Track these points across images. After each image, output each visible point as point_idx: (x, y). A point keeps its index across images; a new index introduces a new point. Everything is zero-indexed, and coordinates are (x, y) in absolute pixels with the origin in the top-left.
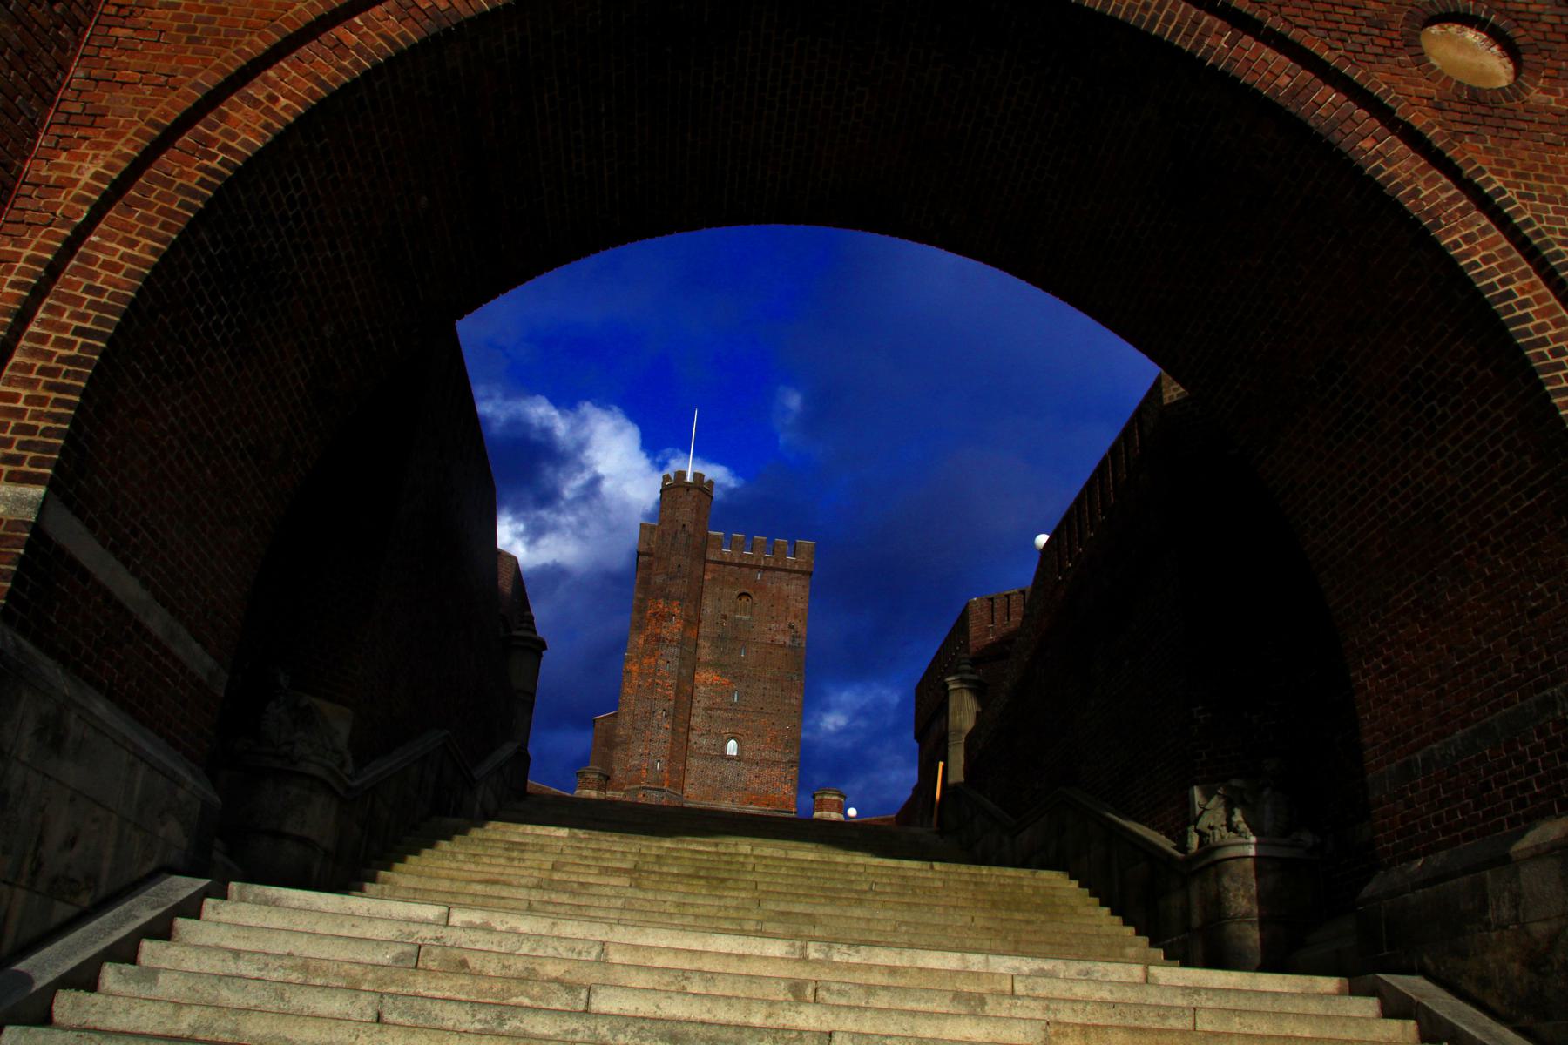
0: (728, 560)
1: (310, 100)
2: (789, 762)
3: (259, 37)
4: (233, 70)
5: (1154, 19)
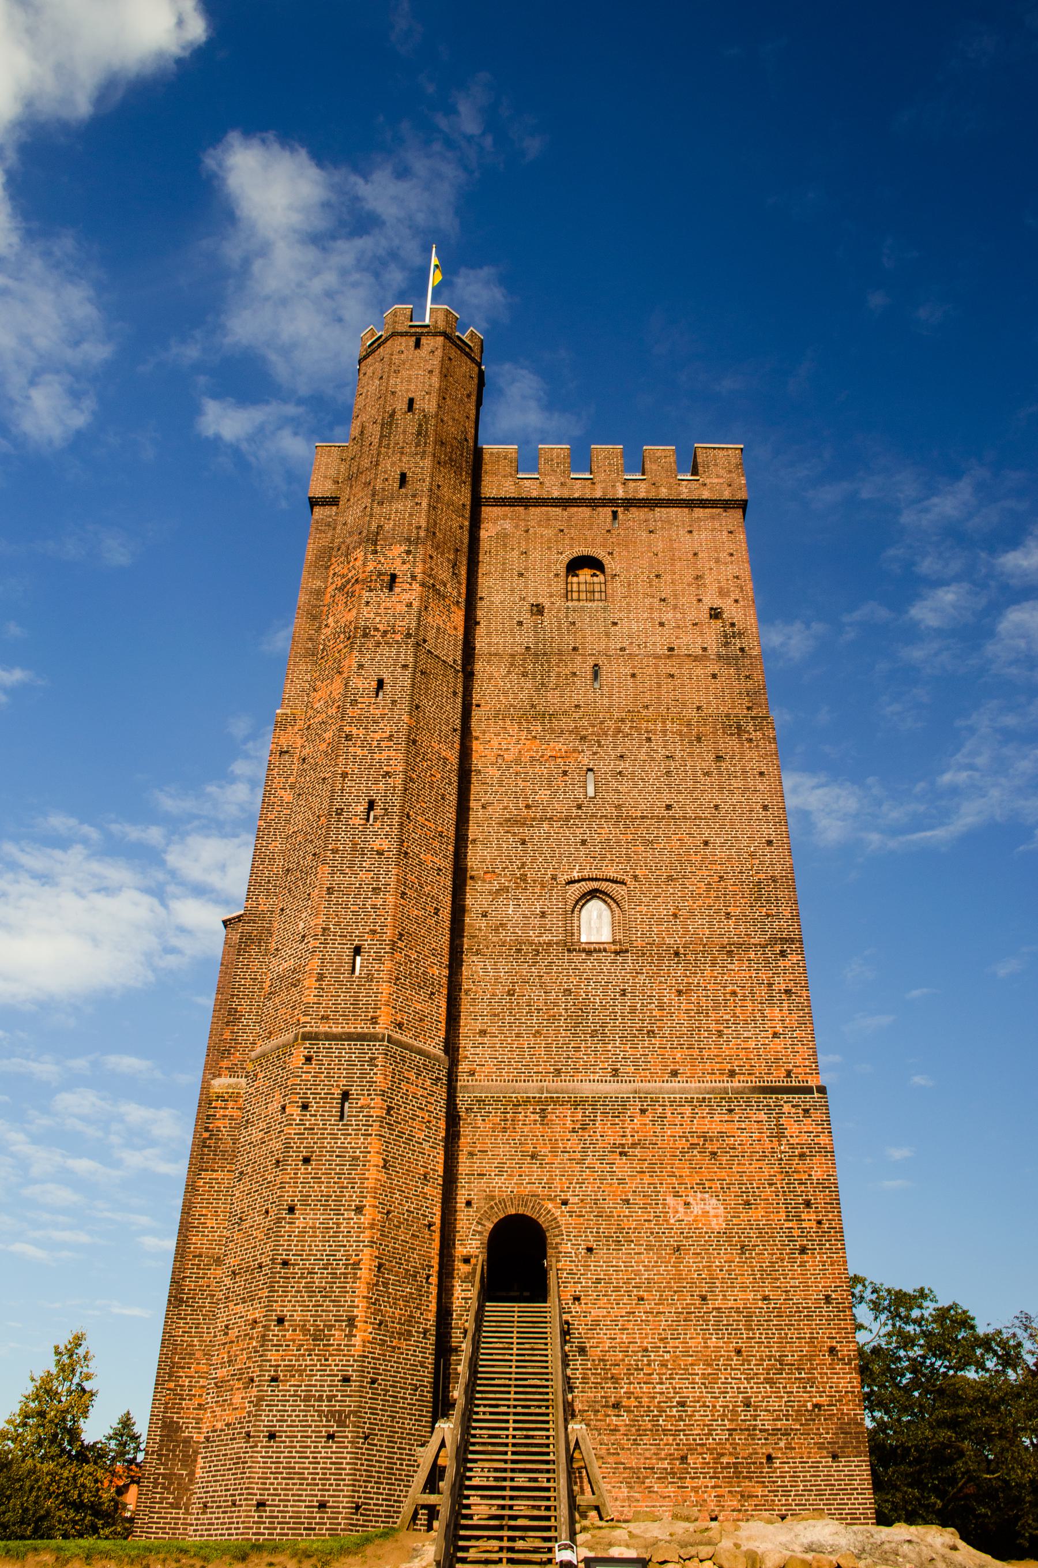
0: (535, 494)
2: (773, 941)
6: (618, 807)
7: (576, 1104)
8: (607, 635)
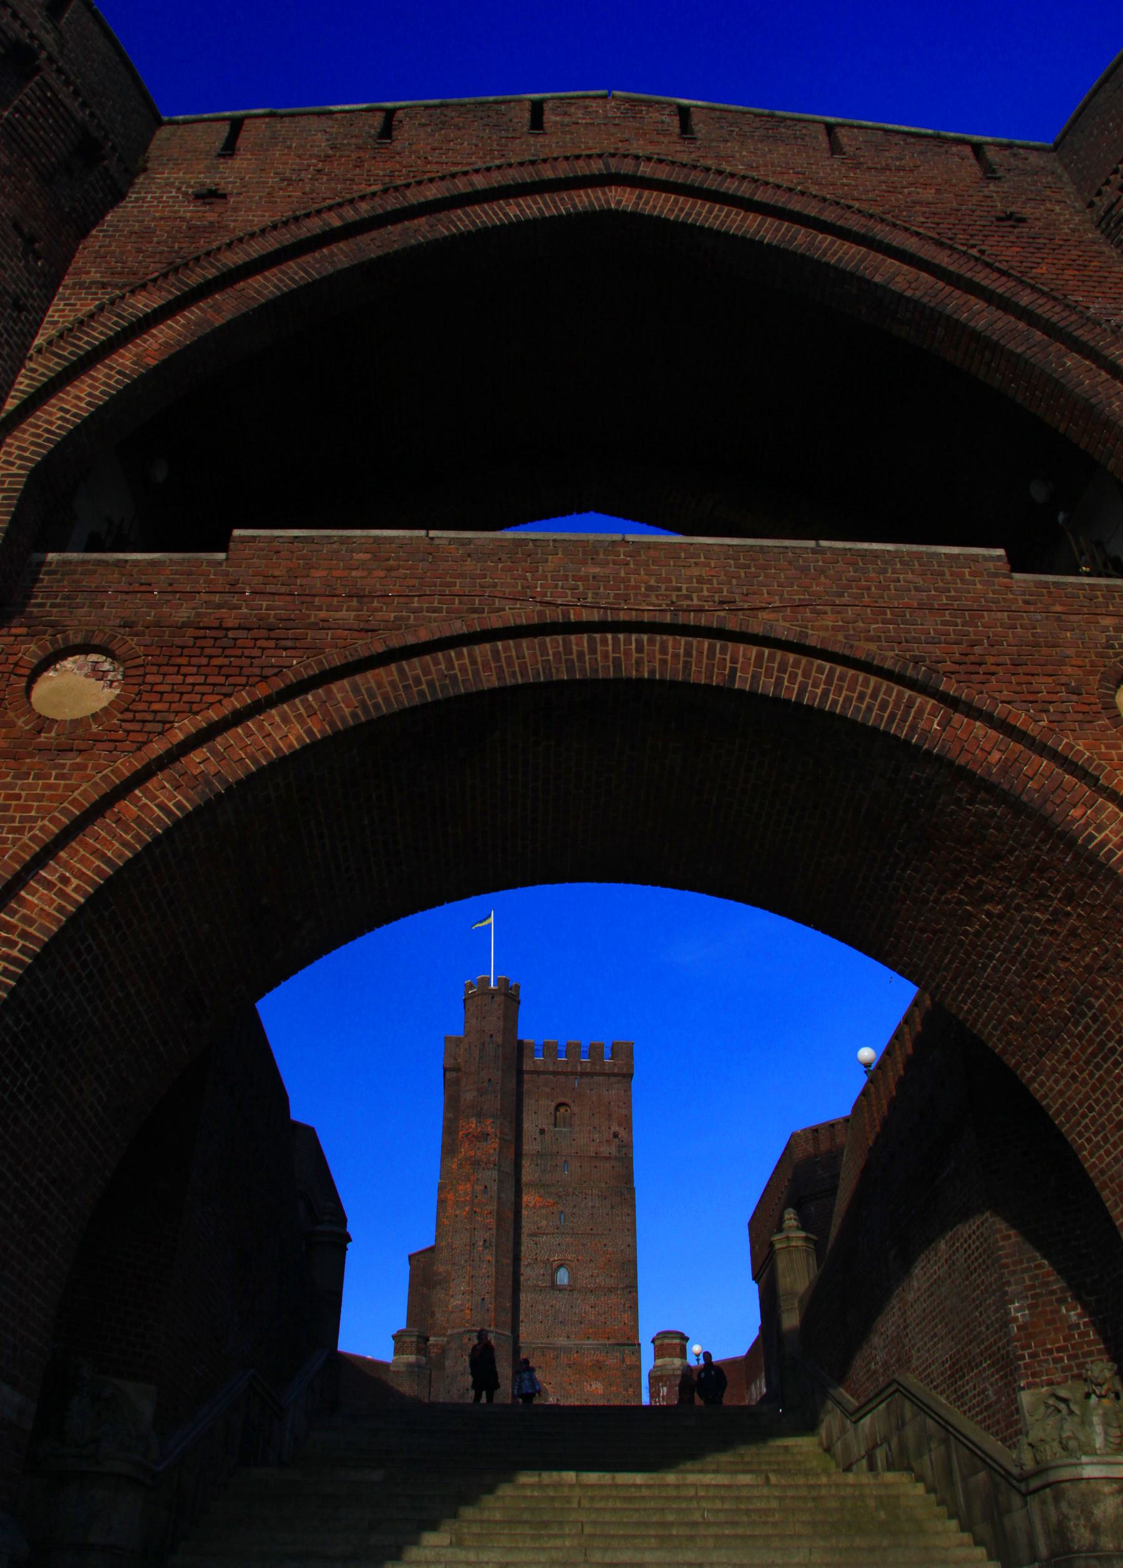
0: (542, 1069)
1: (97, 879)
2: (626, 1287)
3: (50, 821)
4: (28, 858)
5: (869, 709)
6: (572, 1229)
7: (555, 1349)
8: (571, 1145)
